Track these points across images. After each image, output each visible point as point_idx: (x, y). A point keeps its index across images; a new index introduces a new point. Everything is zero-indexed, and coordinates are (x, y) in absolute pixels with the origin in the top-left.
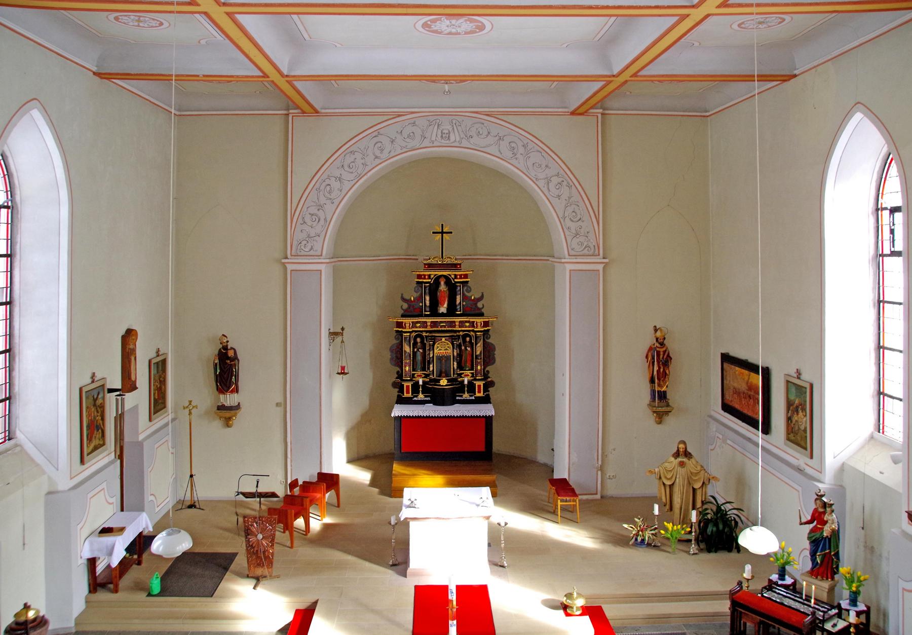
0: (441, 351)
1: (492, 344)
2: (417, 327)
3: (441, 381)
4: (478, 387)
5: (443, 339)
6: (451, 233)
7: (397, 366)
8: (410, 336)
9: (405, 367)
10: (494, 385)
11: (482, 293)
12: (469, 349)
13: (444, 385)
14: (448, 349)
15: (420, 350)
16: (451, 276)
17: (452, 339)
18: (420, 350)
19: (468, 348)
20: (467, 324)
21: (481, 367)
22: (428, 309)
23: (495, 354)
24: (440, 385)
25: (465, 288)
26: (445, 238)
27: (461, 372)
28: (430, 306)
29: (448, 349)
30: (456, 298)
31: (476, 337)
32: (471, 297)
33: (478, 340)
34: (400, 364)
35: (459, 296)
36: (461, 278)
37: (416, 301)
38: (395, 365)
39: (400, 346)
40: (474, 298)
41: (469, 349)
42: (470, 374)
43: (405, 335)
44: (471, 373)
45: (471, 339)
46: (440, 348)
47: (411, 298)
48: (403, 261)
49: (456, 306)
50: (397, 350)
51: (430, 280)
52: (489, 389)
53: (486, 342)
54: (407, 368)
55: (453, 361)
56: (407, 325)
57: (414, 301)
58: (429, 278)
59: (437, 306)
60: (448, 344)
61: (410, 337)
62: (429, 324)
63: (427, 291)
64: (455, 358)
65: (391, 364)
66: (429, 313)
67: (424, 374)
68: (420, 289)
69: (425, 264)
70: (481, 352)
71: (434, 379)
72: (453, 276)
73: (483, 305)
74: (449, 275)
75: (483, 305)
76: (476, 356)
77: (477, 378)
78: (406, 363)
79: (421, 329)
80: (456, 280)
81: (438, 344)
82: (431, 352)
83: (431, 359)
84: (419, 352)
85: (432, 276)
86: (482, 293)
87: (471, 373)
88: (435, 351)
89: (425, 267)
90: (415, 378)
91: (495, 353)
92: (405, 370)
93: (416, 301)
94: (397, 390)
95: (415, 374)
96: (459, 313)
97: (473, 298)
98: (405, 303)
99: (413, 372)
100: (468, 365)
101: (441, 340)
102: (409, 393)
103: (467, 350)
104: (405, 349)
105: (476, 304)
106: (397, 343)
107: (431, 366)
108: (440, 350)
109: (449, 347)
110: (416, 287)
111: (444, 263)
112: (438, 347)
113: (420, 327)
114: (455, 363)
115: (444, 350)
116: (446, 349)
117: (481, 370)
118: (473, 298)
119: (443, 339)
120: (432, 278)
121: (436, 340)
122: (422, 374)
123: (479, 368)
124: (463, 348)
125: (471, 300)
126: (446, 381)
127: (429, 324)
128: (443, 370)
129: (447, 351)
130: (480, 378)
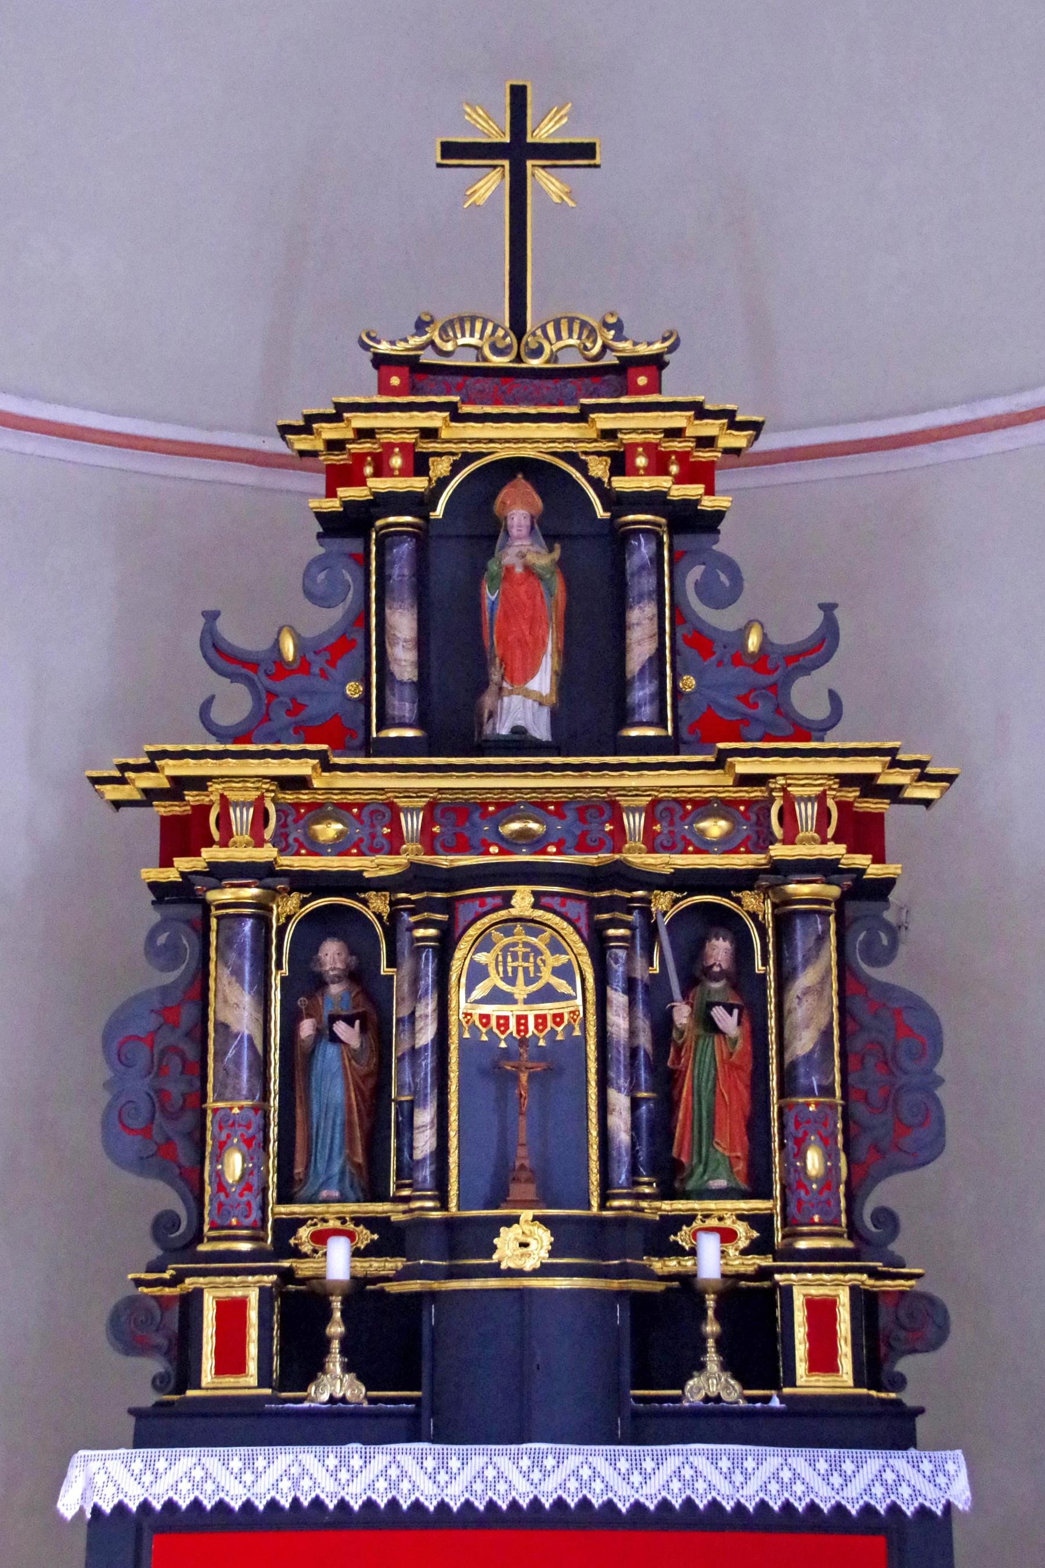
0: (504, 1010)
1: (917, 1005)
2: (316, 849)
3: (506, 1243)
4: (811, 1319)
5: (523, 899)
6: (587, 151)
7: (162, 1174)
8: (262, 907)
9: (218, 1158)
10: (943, 1333)
11: (828, 609)
12: (728, 1022)
13: (529, 1265)
14: (561, 985)
15: (341, 1028)
16: (583, 468)
17: (595, 906)
18: (341, 1028)
19: (718, 1013)
20: (715, 828)
21: (829, 1155)
22: (404, 706)
23: (939, 1081)
24: (495, 1271)
25: (695, 574)
26: (540, 190)
27: (666, 1206)
28: (422, 686)
29: (561, 985)
30: (620, 628)
31: (784, 922)
32: (743, 634)
33: (802, 938)
34: (184, 1154)
35: (650, 609)
36: (659, 465)
37: (318, 663)
38: (142, 1165)
39: (188, 1015)
40: (765, 638)
41: (728, 1022)
42: (741, 1228)
43: (227, 895)
44: (753, 1220)
45: (742, 951)
46: (495, 980)
47: (277, 646)
48: (249, 475)
49: (622, 685)
50: (168, 1038)
51: (419, 484)
52: (904, 1365)
53: (866, 985)
54: (234, 1165)
55: (604, 1084)
56: (241, 818)
57: (303, 665)
58: (419, 465)
59: (482, 684)
60: (556, 948)
61: (263, 922)
62: (411, 824)
63: (401, 570)
64: (620, 1056)
65: (110, 1150)
66: (410, 733)
67: (371, 1223)
68: (348, 575)
69: (380, 361)
70: (827, 1033)
71: (451, 1225)
72: (599, 468)
73: (834, 697)
74: (571, 458)
75: (834, 697)
76: (786, 1076)
77: (802, 1244)
78: (225, 1121)
79: (352, 863)
80: (623, 484)
81: (484, 943)
82: (428, 1007)
83: (428, 1062)
84: (331, 1050)
85: (440, 467)
86: (828, 609)
87: (753, 1220)
88: (460, 1002)
89: (384, 388)
90: (296, 1253)
91: (939, 1069)
92: (219, 1175)
93: (318, 663)
94: (154, 1366)
95: (292, 1225)
96: (651, 732)
97: (753, 642)
98: (233, 677)
99: (283, 1209)
100: (721, 1148)
101: (506, 901)
102: (239, 1368)
103: (712, 1027)
104: (228, 1016)
105: (778, 691)
106: (164, 990)
107: (425, 1117)
108: (496, 996)
109: (564, 972)
110: (318, 563)
111: (535, 363)
112: (477, 973)
113: (340, 848)
114: (619, 1101)
115: (532, 999)
116: (548, 994)
117: (828, 1181)
118: (753, 642)
119: (523, 899)
120: (443, 482)
121: (465, 911)
122: (357, 1221)
123: (814, 1161)
124: (682, 1014)
125: (739, 657)
126: (542, 1240)
127: (411, 824)
128: (522, 1157)
129: (548, 1008)
130: (827, 1244)
